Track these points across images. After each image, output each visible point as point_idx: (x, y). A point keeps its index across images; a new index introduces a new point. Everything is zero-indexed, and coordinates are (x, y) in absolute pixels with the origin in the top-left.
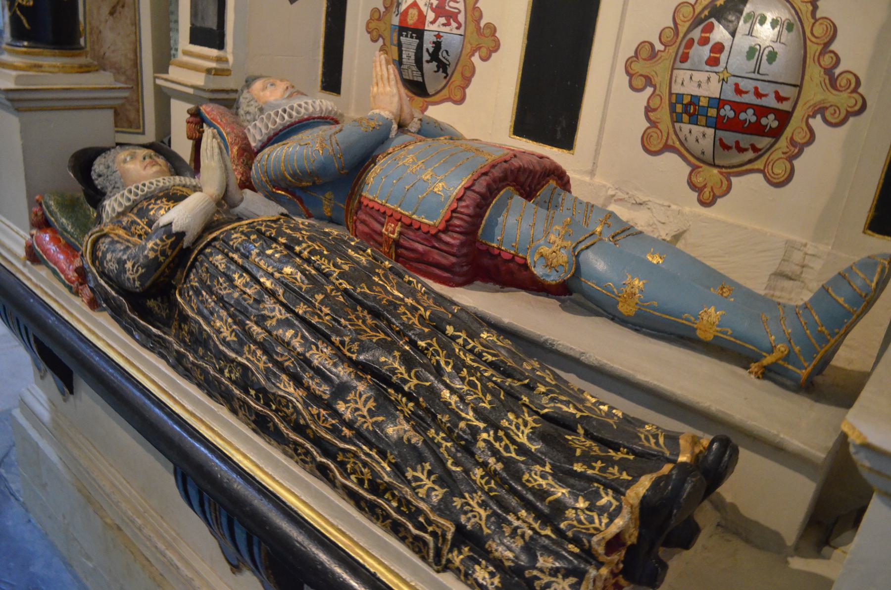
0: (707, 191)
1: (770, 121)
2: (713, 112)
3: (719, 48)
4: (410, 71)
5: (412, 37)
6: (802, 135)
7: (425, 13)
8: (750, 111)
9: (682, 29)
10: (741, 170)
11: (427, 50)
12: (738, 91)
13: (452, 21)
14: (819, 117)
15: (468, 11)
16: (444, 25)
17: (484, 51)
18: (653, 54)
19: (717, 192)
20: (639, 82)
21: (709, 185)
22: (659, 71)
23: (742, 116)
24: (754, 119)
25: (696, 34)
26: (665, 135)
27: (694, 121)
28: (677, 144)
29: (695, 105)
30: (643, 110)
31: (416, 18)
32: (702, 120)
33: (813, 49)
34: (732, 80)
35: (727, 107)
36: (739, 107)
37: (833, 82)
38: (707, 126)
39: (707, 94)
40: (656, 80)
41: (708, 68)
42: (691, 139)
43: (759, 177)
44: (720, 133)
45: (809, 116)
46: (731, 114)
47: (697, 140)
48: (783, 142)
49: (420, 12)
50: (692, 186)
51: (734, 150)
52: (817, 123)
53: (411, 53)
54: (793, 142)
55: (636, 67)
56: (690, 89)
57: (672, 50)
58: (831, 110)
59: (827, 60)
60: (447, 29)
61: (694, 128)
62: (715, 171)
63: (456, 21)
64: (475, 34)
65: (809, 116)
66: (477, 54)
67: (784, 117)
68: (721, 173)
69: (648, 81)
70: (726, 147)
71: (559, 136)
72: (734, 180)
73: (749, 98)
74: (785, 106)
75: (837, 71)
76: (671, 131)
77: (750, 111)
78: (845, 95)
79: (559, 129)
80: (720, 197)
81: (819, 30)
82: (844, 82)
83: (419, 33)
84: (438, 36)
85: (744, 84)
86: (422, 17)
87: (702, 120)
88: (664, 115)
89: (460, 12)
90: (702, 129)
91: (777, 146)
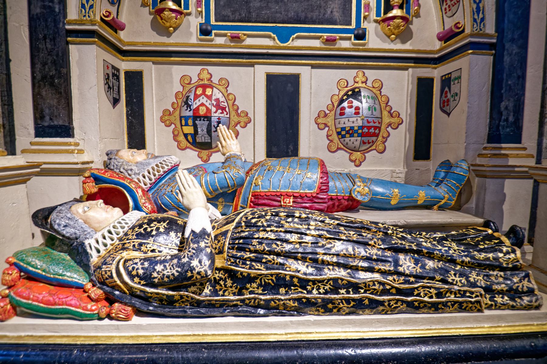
0: (357, 161)
1: (377, 131)
2: (360, 131)
3: (357, 108)
4: (203, 138)
5: (204, 120)
6: (386, 134)
7: (210, 108)
8: (373, 129)
9: (336, 105)
10: (367, 151)
11: (214, 126)
12: (368, 122)
13: (224, 111)
14: (390, 127)
15: (230, 107)
16: (221, 113)
17: (242, 124)
18: (326, 115)
19: (361, 161)
20: (322, 126)
21: (358, 158)
23: (370, 131)
24: (373, 131)
25: (345, 104)
26: (337, 144)
27: (352, 135)
28: (342, 147)
29: (352, 130)
30: (326, 137)
31: (205, 111)
32: (356, 135)
33: (383, 105)
34: (366, 119)
35: (365, 128)
36: (369, 128)
38: (358, 137)
39: (357, 125)
40: (329, 124)
41: (356, 116)
42: (350, 143)
43: (375, 151)
44: (363, 138)
45: (387, 128)
46: (367, 131)
47: (353, 143)
48: (380, 138)
49: (207, 108)
50: (351, 160)
51: (367, 144)
52: (389, 129)
53: (203, 129)
54: (383, 137)
55: (319, 121)
56: (348, 125)
57: (333, 112)
58: (393, 124)
59: (388, 108)
60: (222, 115)
61: (352, 139)
62: (359, 153)
63: (226, 111)
64: (236, 116)
65: (387, 128)
66: (239, 126)
67: (380, 128)
68: (361, 153)
70: (364, 143)
71: (290, 153)
72: (366, 155)
73: (372, 124)
74: (379, 125)
75: (392, 111)
76: (339, 142)
77: (373, 129)
78: (396, 118)
79: (290, 151)
80: (363, 162)
81: (383, 99)
82: (395, 115)
83: (207, 117)
84: (219, 119)
85: (370, 119)
87: (356, 135)
88: (335, 137)
89: (226, 107)
90: (356, 138)
91: (378, 140)
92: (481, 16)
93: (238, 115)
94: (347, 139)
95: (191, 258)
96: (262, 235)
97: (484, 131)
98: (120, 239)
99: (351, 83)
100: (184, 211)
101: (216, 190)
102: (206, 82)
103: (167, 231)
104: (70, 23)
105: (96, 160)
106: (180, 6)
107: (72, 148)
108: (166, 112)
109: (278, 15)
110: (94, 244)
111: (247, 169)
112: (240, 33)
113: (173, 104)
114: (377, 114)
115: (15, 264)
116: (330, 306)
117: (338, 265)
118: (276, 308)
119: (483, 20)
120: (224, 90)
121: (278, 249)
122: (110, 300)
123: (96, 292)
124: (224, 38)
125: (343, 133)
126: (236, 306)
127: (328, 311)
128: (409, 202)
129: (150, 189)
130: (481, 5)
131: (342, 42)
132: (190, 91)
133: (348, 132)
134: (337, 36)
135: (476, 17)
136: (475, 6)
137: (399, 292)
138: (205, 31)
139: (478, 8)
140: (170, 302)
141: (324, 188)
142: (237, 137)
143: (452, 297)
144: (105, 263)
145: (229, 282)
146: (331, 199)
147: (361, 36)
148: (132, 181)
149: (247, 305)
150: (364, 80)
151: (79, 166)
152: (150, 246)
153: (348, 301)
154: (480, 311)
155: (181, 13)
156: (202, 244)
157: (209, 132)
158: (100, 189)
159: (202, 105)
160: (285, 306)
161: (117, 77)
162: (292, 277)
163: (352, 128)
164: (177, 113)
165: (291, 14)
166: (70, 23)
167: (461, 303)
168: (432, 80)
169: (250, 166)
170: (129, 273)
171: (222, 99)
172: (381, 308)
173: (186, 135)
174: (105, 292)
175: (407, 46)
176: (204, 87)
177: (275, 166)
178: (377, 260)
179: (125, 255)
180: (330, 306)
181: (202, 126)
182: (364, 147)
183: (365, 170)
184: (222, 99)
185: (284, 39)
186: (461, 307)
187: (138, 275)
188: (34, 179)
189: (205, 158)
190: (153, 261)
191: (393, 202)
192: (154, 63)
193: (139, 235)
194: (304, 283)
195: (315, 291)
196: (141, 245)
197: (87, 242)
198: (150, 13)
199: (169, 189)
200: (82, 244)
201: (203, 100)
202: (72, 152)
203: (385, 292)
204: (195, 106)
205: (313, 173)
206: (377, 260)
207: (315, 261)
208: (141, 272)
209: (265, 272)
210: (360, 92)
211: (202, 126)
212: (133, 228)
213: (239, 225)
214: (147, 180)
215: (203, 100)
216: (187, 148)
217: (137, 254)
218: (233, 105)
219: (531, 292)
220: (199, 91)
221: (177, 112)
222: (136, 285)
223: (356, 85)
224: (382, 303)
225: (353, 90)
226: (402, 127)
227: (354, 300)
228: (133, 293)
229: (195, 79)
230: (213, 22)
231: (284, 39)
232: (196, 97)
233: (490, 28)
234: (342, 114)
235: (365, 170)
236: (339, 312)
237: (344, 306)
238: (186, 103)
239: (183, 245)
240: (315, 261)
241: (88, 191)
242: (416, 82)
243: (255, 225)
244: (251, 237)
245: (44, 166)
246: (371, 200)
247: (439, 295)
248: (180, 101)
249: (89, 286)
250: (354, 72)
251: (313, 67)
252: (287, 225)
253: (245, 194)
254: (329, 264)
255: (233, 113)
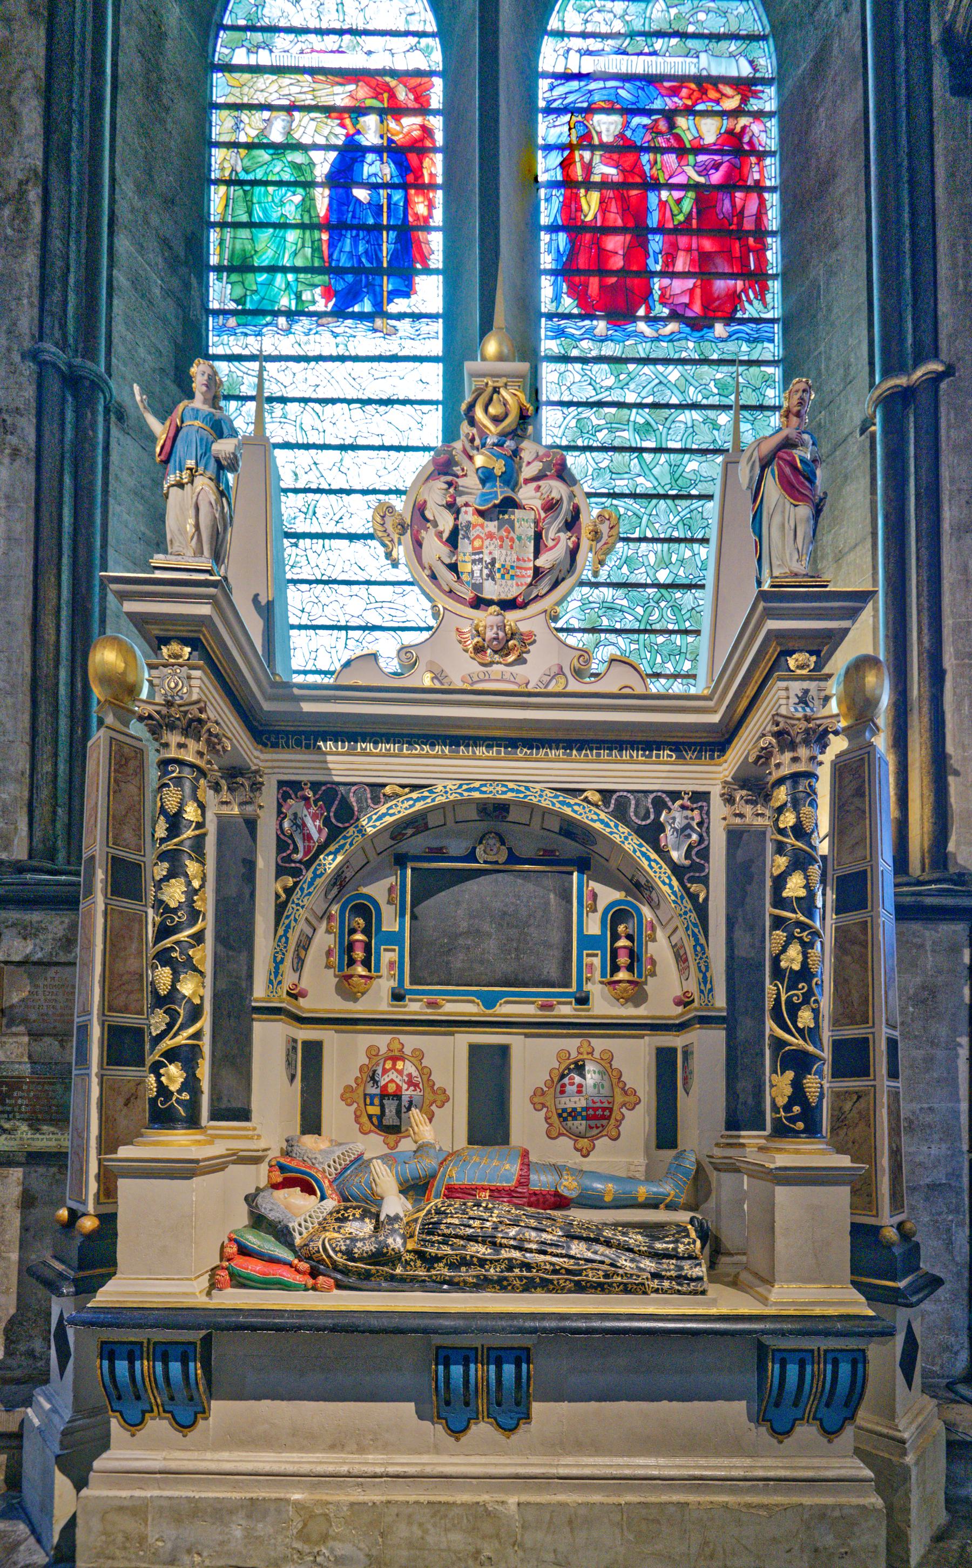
1: (607, 1113)
2: (584, 1114)
3: (580, 1086)
9: (556, 1080)
12: (594, 1102)
17: (439, 1103)
20: (539, 1107)
22: (549, 1100)
25: (566, 1080)
27: (575, 1118)
33: (615, 1081)
36: (595, 1109)
37: (626, 1093)
40: (548, 1104)
48: (612, 1121)
49: (398, 1085)
52: (624, 1110)
55: (536, 1100)
59: (621, 1085)
67: (611, 1110)
69: (544, 1105)
70: (591, 1128)
73: (599, 1105)
83: (397, 1096)
86: (399, 1087)
92: (709, 986)
93: (434, 1092)
94: (570, 1123)
95: (387, 1236)
96: (449, 1220)
97: (721, 1115)
98: (320, 1224)
99: (574, 1054)
100: (378, 1201)
101: (407, 1181)
102: (397, 1054)
103: (362, 1218)
104: (256, 1001)
105: (273, 1147)
106: (370, 971)
107: (250, 1133)
108: (348, 1089)
109: (483, 977)
110: (297, 1227)
111: (441, 1160)
112: (439, 998)
113: (357, 1078)
114: (604, 1092)
115: (236, 1241)
116: (505, 1283)
117: (515, 1248)
118: (458, 1284)
119: (711, 990)
120: (417, 1063)
121: (461, 1233)
122: (314, 1274)
123: (304, 1266)
124: (419, 1004)
125: (565, 1115)
126: (424, 1281)
127: (504, 1289)
128: (626, 1199)
129: (335, 1179)
130: (708, 974)
131: (562, 1007)
132: (377, 1065)
133: (570, 1114)
134: (554, 1001)
135: (702, 987)
136: (701, 976)
137: (569, 1272)
138: (397, 996)
139: (705, 977)
140: (367, 1276)
141: (524, 1181)
142: (430, 1120)
143: (619, 1279)
144: (312, 1240)
145: (419, 1263)
146: (535, 1194)
147: (583, 1000)
148: (318, 1170)
149: (434, 1281)
150: (590, 1050)
151: (260, 1154)
152: (348, 1230)
153: (521, 1278)
154: (645, 1293)
155: (371, 978)
156: (396, 1226)
157: (398, 1113)
158: (285, 1179)
159: (392, 1081)
160: (465, 1282)
161: (295, 1049)
162: (472, 1257)
163: (574, 1110)
164: (360, 1091)
165: (499, 975)
166: (256, 1001)
167: (625, 1284)
168: (674, 1050)
169: (444, 1156)
170: (333, 1249)
171: (415, 1073)
172: (551, 1287)
173: (370, 1117)
174: (311, 1267)
175: (642, 1011)
176: (395, 1059)
177: (471, 1157)
178: (551, 1245)
179: (329, 1235)
180: (505, 1283)
181: (391, 1106)
182: (595, 1131)
183: (591, 1163)
184: (415, 1073)
185: (490, 1002)
186: (626, 1289)
187: (341, 1251)
188: (231, 1166)
189: (392, 1144)
190: (354, 1240)
191: (607, 1199)
192: (337, 1031)
193: (337, 1220)
194: (482, 1262)
195: (492, 1271)
196: (340, 1228)
197: (291, 1225)
198: (336, 976)
199: (357, 1179)
200: (287, 1227)
201: (393, 1075)
202: (252, 1138)
203: (555, 1272)
204: (382, 1083)
205: (512, 1164)
206: (551, 1245)
207: (494, 1244)
208: (343, 1248)
209: (450, 1252)
210: (584, 1065)
211: (391, 1106)
212: (331, 1213)
213: (429, 1212)
214: (333, 1170)
215: (393, 1075)
216: (370, 1131)
217: (336, 1235)
218: (429, 1080)
219: (699, 1279)
220: (389, 1065)
221: (361, 1089)
222: (339, 1258)
223: (581, 1057)
224: (551, 1281)
225: (576, 1063)
226: (640, 1108)
227: (526, 1278)
228: (335, 1267)
229: (383, 1050)
230: (407, 985)
231: (490, 1002)
232: (385, 1071)
233: (720, 1001)
234: (562, 1092)
235: (591, 1163)
236: (514, 1290)
237: (517, 1283)
238: (373, 1078)
239: (376, 1228)
240: (494, 1244)
241: (274, 1181)
242: (654, 1052)
243: (444, 1213)
244: (439, 1223)
245: (241, 1154)
246: (580, 1196)
247: (606, 1276)
248: (365, 1076)
249: (296, 1261)
250: (577, 1042)
251: (526, 1035)
252: (471, 1213)
253: (439, 1185)
254: (506, 1246)
255: (428, 1090)
